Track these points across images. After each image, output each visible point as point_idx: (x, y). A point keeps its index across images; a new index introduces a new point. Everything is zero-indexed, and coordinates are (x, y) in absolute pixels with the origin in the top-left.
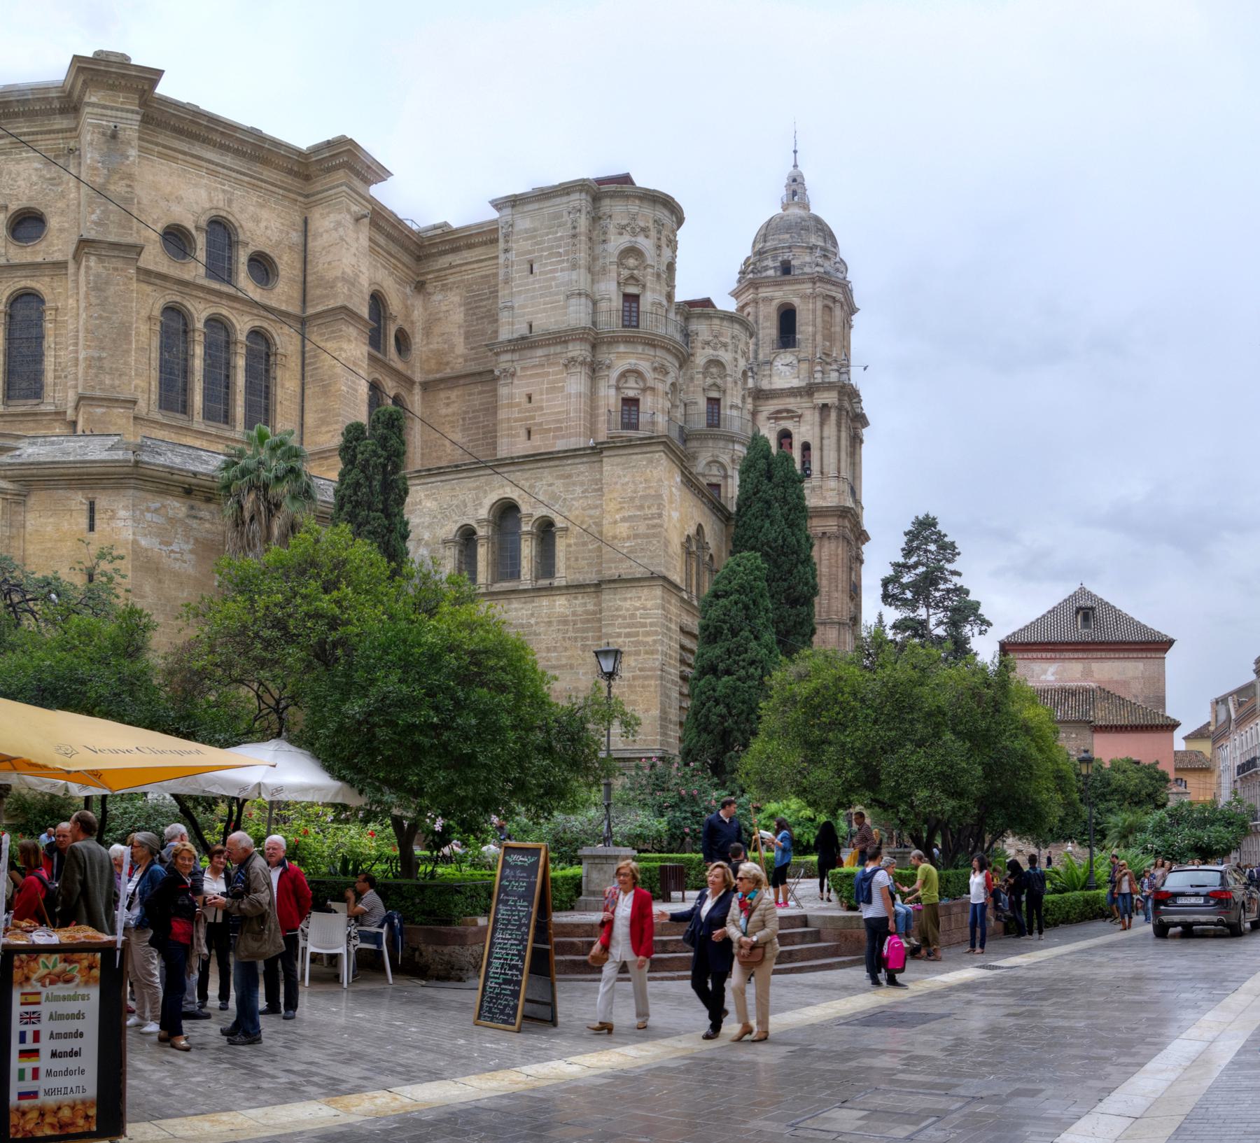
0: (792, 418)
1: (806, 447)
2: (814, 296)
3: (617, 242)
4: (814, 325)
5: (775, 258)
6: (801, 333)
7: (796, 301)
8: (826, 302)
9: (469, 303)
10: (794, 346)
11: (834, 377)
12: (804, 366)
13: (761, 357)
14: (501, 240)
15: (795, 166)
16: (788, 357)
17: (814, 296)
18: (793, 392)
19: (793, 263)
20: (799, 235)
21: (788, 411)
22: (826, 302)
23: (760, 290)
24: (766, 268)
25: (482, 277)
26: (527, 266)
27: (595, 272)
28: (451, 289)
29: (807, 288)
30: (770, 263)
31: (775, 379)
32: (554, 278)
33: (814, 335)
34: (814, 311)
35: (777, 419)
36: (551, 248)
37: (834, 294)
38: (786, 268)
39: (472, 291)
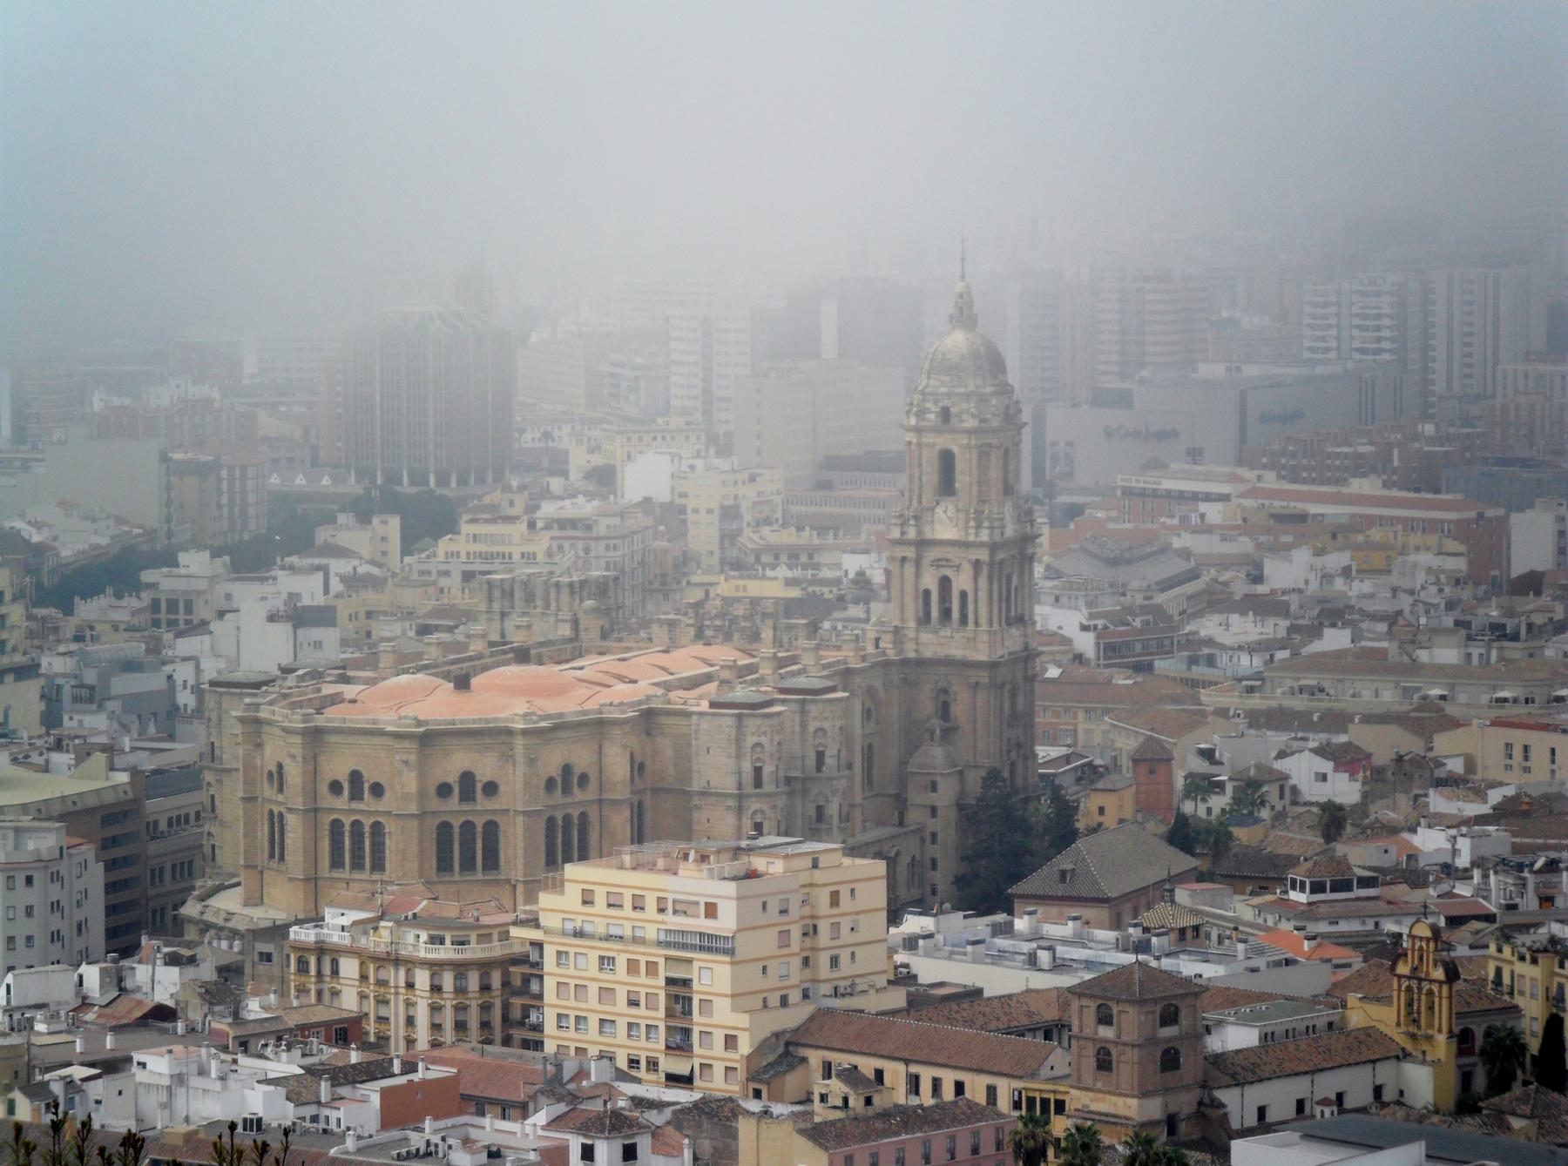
1: (964, 595)
3: (750, 740)
7: (955, 449)
13: (924, 501)
17: (968, 446)
21: (948, 560)
27: (739, 756)
31: (937, 526)
35: (938, 566)
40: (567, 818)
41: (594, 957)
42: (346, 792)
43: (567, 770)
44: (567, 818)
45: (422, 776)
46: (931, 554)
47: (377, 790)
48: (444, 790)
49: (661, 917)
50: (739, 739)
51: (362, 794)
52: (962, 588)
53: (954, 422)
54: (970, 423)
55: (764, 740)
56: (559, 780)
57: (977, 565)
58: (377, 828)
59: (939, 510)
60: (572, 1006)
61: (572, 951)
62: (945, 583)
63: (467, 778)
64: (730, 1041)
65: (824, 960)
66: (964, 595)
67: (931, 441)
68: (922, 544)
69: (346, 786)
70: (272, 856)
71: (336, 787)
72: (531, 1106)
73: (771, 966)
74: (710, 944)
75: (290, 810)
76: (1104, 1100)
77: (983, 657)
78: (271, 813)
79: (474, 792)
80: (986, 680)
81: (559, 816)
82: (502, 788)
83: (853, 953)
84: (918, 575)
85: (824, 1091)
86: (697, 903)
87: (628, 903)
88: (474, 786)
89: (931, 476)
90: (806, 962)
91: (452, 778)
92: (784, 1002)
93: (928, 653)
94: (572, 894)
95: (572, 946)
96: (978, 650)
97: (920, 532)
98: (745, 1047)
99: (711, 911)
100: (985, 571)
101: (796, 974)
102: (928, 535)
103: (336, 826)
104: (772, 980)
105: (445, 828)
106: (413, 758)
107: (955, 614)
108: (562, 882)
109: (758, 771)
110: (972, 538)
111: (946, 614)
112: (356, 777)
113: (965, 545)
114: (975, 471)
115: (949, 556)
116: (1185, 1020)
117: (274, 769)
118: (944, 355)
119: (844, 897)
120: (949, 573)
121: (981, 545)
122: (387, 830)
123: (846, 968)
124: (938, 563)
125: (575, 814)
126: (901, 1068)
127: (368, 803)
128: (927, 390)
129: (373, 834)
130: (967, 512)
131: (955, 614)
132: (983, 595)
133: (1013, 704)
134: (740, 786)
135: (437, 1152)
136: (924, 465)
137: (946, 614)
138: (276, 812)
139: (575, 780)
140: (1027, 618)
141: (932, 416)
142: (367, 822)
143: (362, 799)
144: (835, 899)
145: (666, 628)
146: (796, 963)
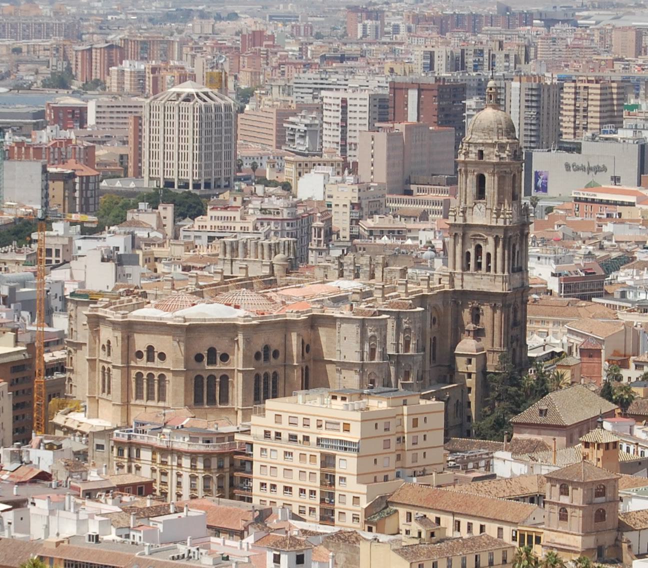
1: (489, 255)
13: (468, 202)
27: (362, 343)
40: (266, 375)
41: (281, 452)
42: (145, 357)
43: (267, 348)
44: (266, 375)
45: (186, 349)
46: (471, 233)
47: (162, 356)
49: (318, 431)
53: (486, 159)
54: (495, 160)
56: (262, 353)
57: (497, 240)
58: (162, 377)
60: (269, 480)
61: (269, 448)
62: (478, 249)
64: (356, 499)
65: (409, 456)
66: (489, 255)
68: (466, 227)
69: (145, 354)
70: (104, 391)
71: (139, 355)
72: (246, 533)
73: (379, 458)
74: (345, 446)
75: (114, 367)
76: (563, 537)
77: (500, 291)
78: (104, 368)
79: (216, 359)
81: (262, 374)
82: (231, 357)
83: (425, 453)
84: (463, 244)
85: (408, 529)
86: (338, 424)
87: (300, 422)
90: (399, 457)
92: (386, 479)
93: (468, 288)
94: (270, 416)
95: (269, 444)
96: (495, 286)
97: (465, 220)
98: (364, 504)
99: (347, 427)
101: (392, 463)
102: (469, 222)
103: (139, 375)
104: (379, 467)
105: (199, 379)
107: (484, 265)
108: (264, 410)
110: (494, 224)
111: (478, 266)
112: (150, 349)
113: (491, 227)
114: (496, 186)
116: (609, 495)
117: (106, 344)
119: (421, 422)
122: (167, 379)
123: (421, 461)
124: (475, 238)
125: (271, 372)
126: (450, 518)
127: (157, 363)
128: (470, 141)
129: (159, 381)
131: (484, 265)
132: (499, 255)
133: (515, 316)
134: (362, 359)
135: (194, 557)
137: (478, 266)
138: (106, 368)
139: (272, 353)
140: (523, 268)
141: (473, 155)
142: (156, 374)
144: (415, 423)
145: (322, 270)
146: (393, 457)
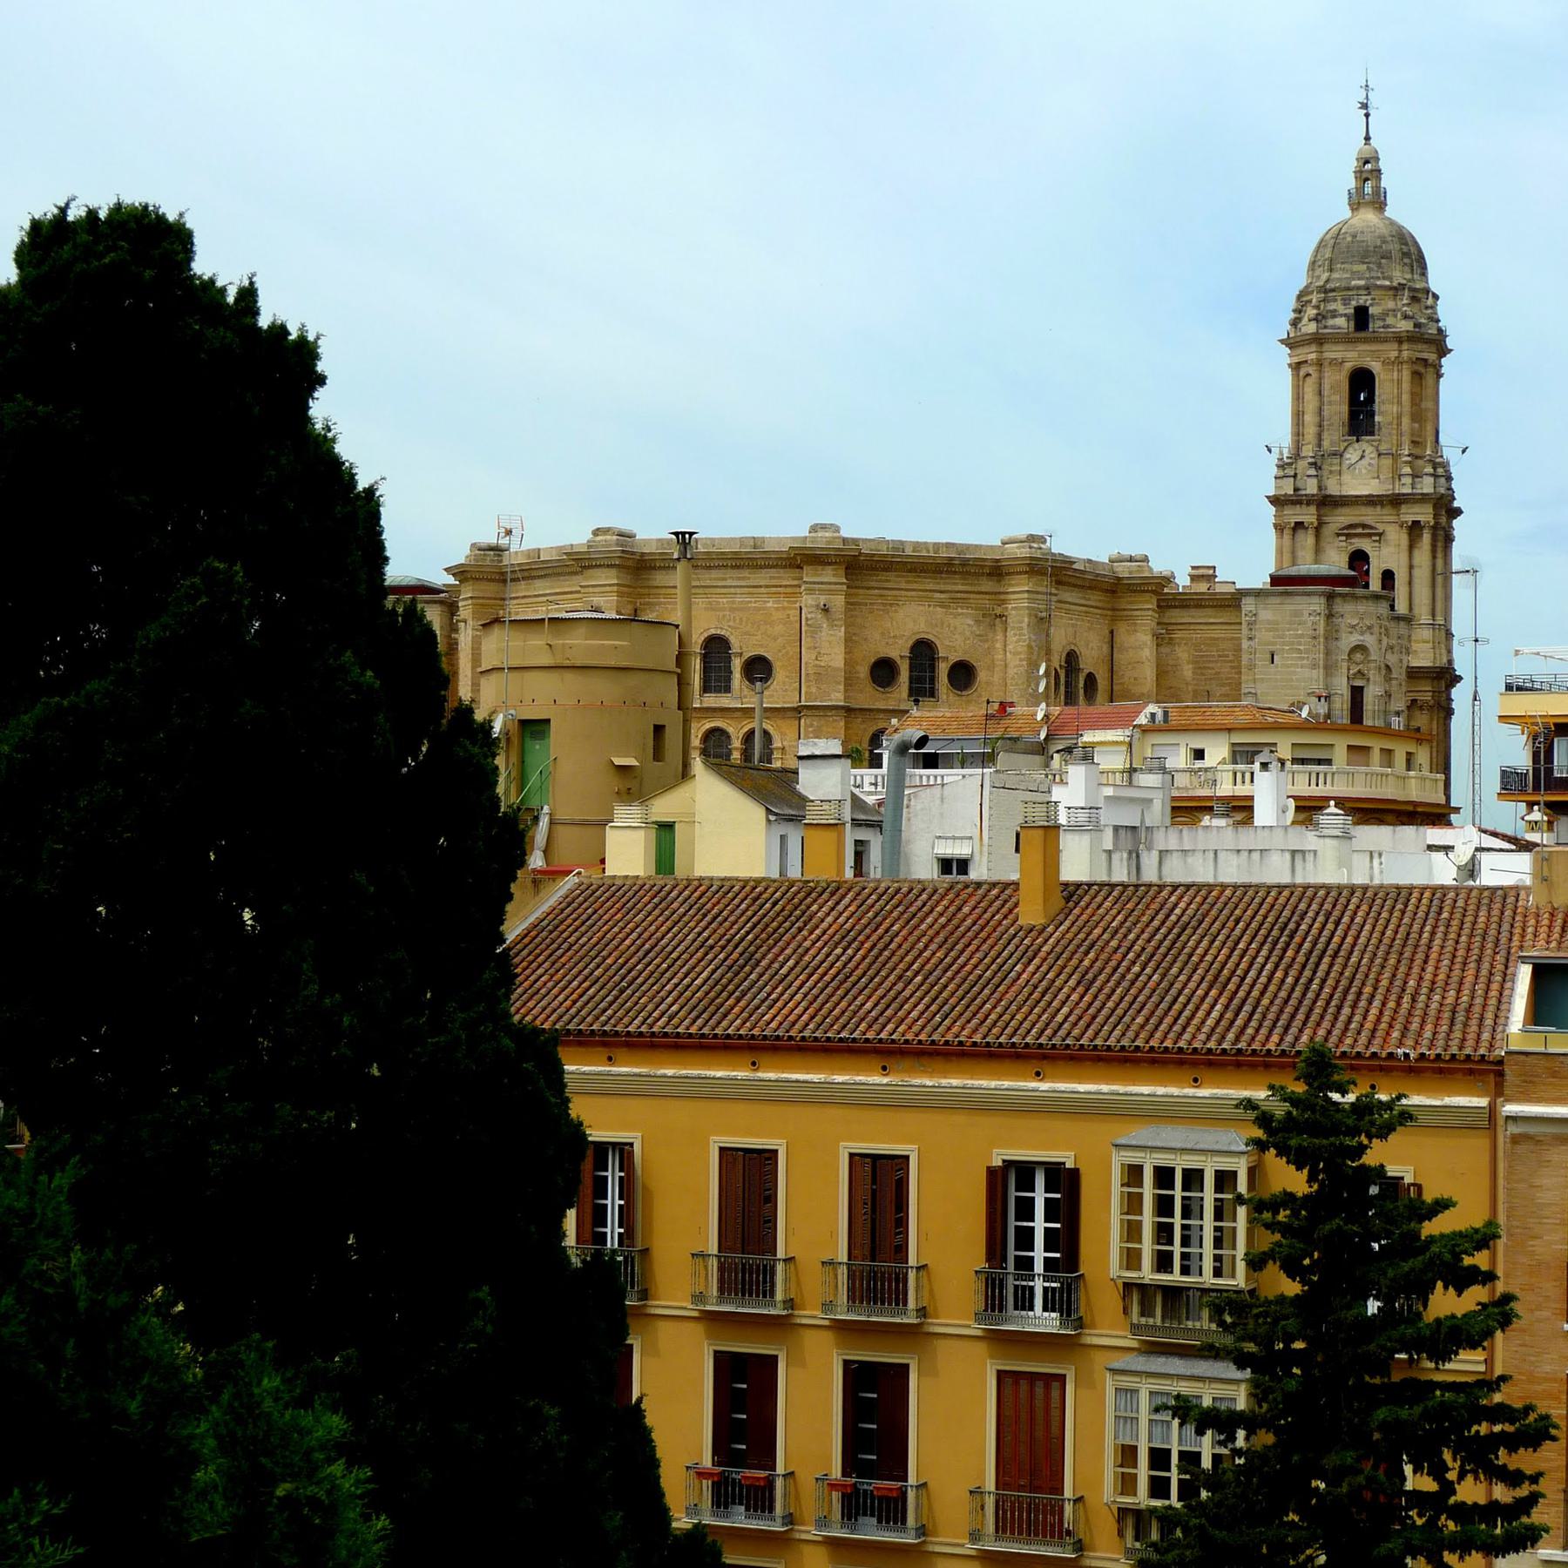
0: (1370, 535)
2: (1398, 362)
3: (1349, 640)
4: (1400, 403)
5: (1346, 302)
6: (1381, 413)
7: (1376, 367)
8: (1416, 367)
9: (1197, 662)
10: (1372, 434)
11: (1427, 485)
12: (1387, 462)
13: (1326, 444)
14: (1244, 626)
15: (1367, 138)
16: (1366, 446)
17: (1398, 362)
18: (1371, 501)
19: (1371, 311)
20: (1379, 265)
21: (1364, 526)
22: (1416, 367)
23: (1326, 347)
24: (1334, 314)
25: (1211, 639)
26: (1269, 656)
27: (1329, 669)
28: (1179, 644)
29: (1391, 351)
30: (1337, 306)
31: (1346, 477)
32: (1295, 673)
33: (1399, 417)
34: (1399, 382)
35: (1348, 536)
36: (1293, 643)
37: (1425, 355)
38: (1361, 317)
39: (1201, 651)
45: (849, 642)
46: (1341, 518)
47: (759, 669)
48: (883, 671)
50: (1331, 635)
51: (729, 679)
52: (1385, 566)
55: (1369, 640)
57: (1415, 529)
59: (1352, 455)
63: (923, 652)
67: (1338, 355)
68: (1326, 502)
79: (933, 680)
80: (1428, 697)
82: (982, 676)
88: (933, 668)
89: (1338, 408)
91: (899, 651)
100: (1427, 537)
102: (1333, 489)
106: (838, 602)
109: (1357, 694)
113: (1396, 501)
114: (1406, 397)
115: (1369, 520)
118: (1354, 236)
120: (1365, 545)
121: (1423, 498)
124: (1348, 532)
127: (740, 693)
128: (1330, 286)
130: (1395, 457)
136: (1326, 393)
143: (728, 689)
